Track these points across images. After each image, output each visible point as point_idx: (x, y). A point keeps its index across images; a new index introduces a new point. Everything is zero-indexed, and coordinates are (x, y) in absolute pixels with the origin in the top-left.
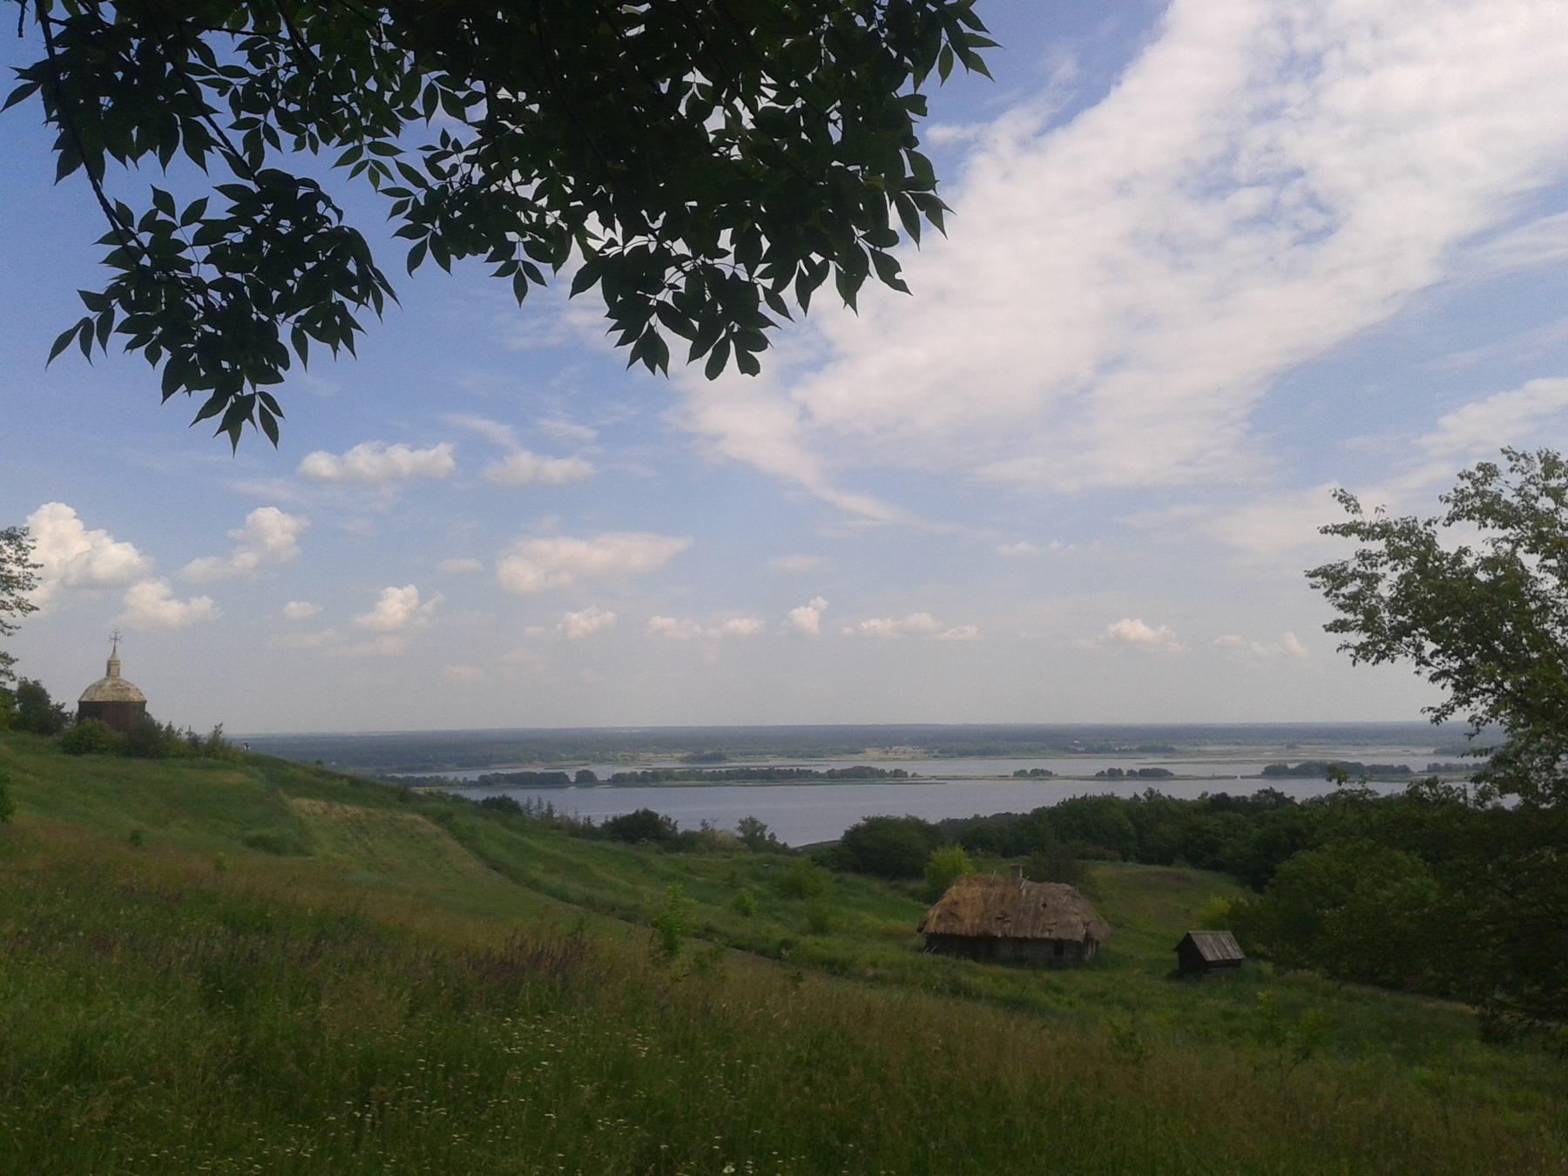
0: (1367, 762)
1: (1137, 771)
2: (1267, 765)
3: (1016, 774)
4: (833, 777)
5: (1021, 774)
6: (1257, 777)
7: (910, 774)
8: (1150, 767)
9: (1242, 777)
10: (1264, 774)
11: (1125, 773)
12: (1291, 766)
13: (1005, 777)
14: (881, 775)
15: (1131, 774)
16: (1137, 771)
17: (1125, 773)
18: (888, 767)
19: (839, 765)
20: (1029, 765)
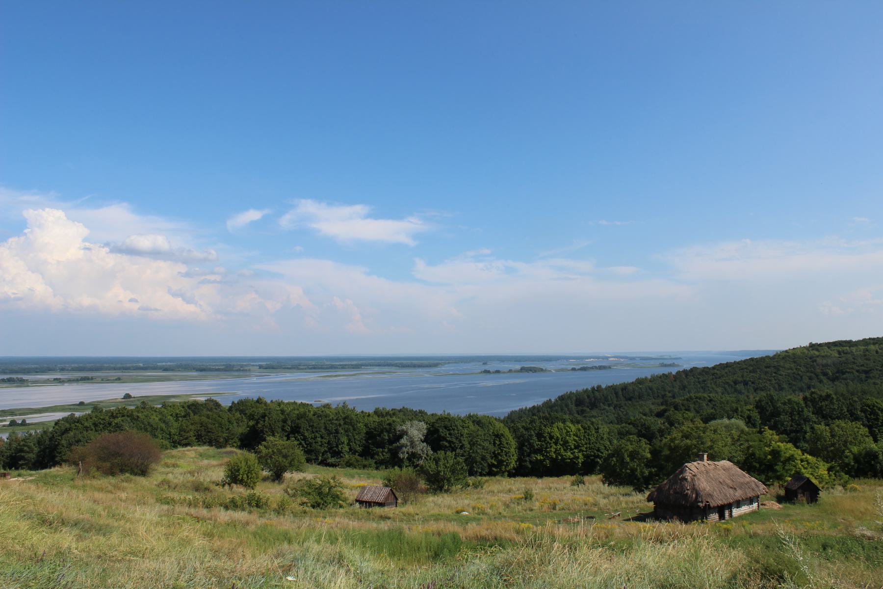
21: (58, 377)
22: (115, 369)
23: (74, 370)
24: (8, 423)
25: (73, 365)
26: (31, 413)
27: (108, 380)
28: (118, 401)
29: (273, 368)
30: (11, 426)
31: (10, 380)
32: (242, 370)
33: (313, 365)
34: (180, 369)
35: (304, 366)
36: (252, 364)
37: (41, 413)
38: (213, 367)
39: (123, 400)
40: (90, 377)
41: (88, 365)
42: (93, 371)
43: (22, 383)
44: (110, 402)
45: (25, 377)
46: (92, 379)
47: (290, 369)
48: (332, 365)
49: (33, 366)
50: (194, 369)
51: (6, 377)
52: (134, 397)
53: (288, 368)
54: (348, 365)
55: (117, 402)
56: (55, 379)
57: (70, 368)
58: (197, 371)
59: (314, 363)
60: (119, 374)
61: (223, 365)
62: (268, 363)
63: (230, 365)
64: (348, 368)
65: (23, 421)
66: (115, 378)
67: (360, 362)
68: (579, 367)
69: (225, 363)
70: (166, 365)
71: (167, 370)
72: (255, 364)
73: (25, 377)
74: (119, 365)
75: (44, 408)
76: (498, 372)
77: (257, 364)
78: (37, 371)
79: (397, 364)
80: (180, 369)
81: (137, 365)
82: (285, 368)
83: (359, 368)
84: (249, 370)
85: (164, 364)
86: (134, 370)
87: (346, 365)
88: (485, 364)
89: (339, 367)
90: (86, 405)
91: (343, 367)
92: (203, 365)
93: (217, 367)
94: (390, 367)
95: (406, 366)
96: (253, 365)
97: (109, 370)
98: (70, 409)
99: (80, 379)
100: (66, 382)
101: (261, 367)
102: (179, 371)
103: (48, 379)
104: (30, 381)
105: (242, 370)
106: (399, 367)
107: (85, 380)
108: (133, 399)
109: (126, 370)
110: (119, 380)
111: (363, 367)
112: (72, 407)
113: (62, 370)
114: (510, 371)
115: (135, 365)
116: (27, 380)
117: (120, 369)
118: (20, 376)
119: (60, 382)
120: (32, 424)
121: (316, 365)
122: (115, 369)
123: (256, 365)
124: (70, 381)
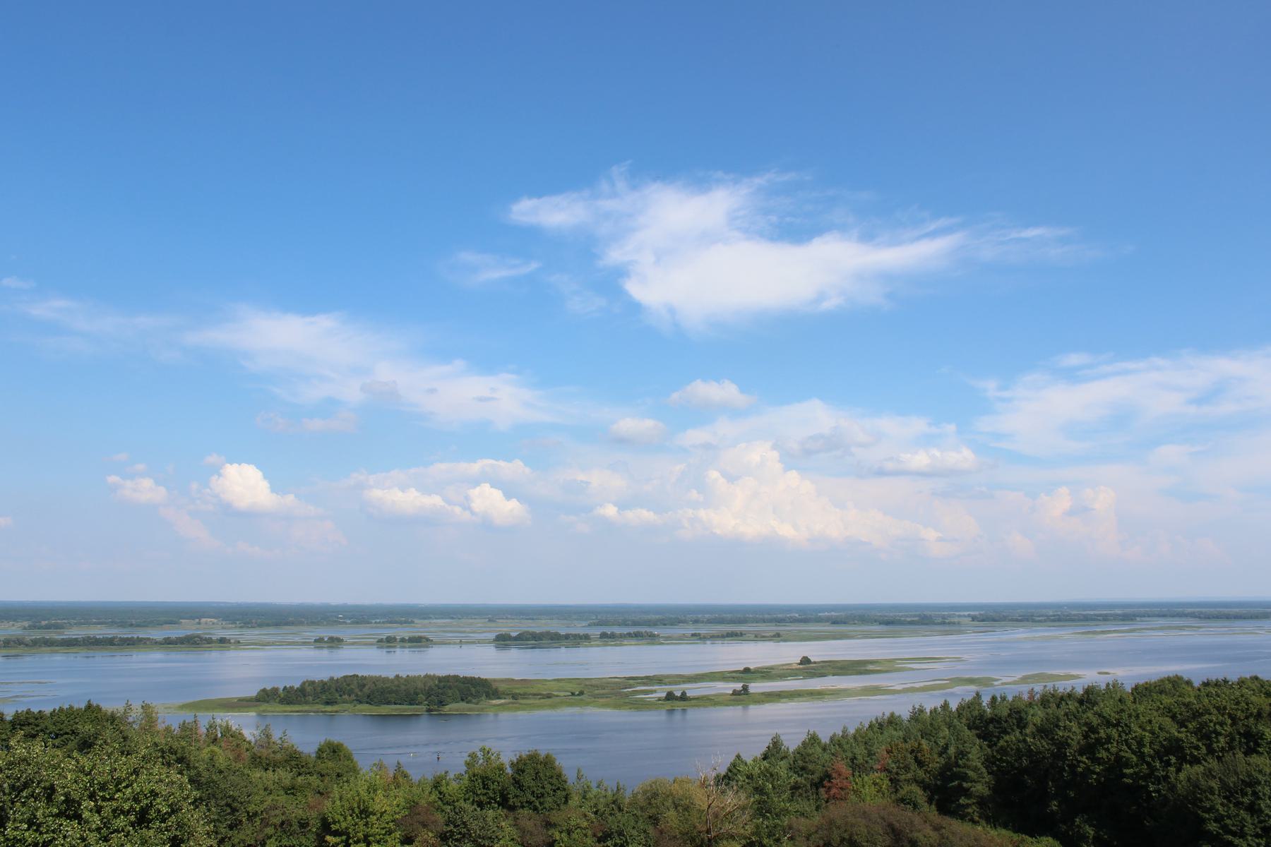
0: (538, 631)
1: (407, 638)
2: (497, 634)
3: (316, 641)
4: (168, 643)
7: (232, 641)
10: (495, 640)
11: (398, 640)
12: (514, 634)
14: (209, 641)
15: (403, 640)
16: (407, 638)
19: (175, 633)
20: (326, 632)
21: (697, 632)
22: (764, 622)
23: (710, 622)
24: (664, 695)
25: (707, 616)
26: (684, 682)
27: (764, 637)
28: (794, 668)
29: (994, 620)
30: (669, 700)
31: (637, 635)
32: (949, 623)
33: (1054, 616)
34: (856, 622)
35: (1039, 616)
36: (957, 613)
37: (696, 682)
38: (903, 619)
39: (801, 666)
40: (739, 632)
41: (729, 616)
42: (735, 623)
43: (652, 639)
44: (783, 669)
46: (741, 635)
47: (1021, 621)
48: (1084, 615)
49: (657, 617)
50: (875, 621)
51: (632, 630)
52: (815, 663)
53: (1017, 620)
54: (1111, 615)
55: (793, 669)
56: (693, 635)
57: (705, 620)
58: (880, 624)
59: (1051, 613)
60: (771, 629)
61: (915, 616)
62: (982, 612)
63: (925, 616)
64: (1115, 620)
65: (682, 694)
66: (772, 634)
67: (1128, 611)
69: (917, 613)
70: (832, 616)
71: (838, 623)
72: (962, 613)
74: (766, 616)
75: (697, 675)
77: (966, 613)
78: (663, 623)
79: (1194, 613)
80: (856, 622)
81: (792, 615)
82: (1012, 620)
83: (1132, 620)
84: (959, 623)
85: (826, 613)
86: (791, 622)
87: (1106, 615)
89: (1099, 618)
90: (753, 673)
91: (1105, 618)
92: (886, 616)
93: (909, 619)
94: (1184, 619)
95: (1214, 617)
96: (959, 616)
97: (757, 622)
98: (734, 678)
99: (725, 634)
100: (709, 639)
101: (974, 618)
102: (855, 624)
103: (684, 634)
104: (662, 637)
105: (949, 623)
106: (1200, 618)
107: (732, 636)
108: (814, 665)
109: (776, 621)
110: (777, 637)
111: (1138, 619)
112: (734, 674)
113: (696, 621)
115: (788, 615)
116: (658, 635)
117: (771, 621)
118: (649, 630)
119: (700, 639)
120: (694, 699)
121: (1058, 615)
122: (764, 621)
123: (965, 616)
124: (713, 637)
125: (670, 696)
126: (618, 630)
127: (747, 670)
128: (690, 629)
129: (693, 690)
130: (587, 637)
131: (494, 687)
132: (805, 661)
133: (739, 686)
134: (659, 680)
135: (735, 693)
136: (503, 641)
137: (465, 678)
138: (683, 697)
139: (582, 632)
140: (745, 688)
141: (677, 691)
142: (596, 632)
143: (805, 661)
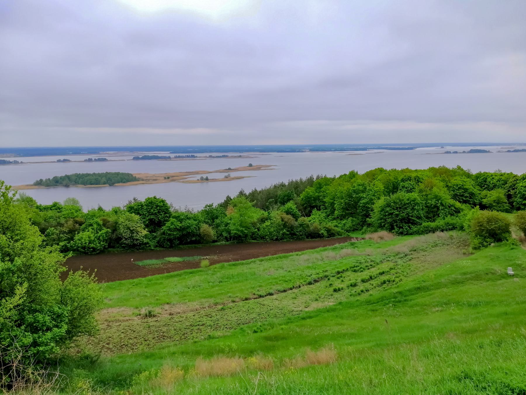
5: (59, 161)
6: (131, 160)
8: (101, 158)
9: (127, 160)
12: (140, 157)
13: (54, 162)
14: (9, 163)
17: (93, 160)
18: (12, 159)
20: (62, 158)
45: (195, 155)
46: (227, 156)
60: (239, 154)
68: (513, 150)
73: (195, 155)
76: (456, 152)
88: (442, 147)
113: (211, 151)
114: (464, 152)
116: (197, 156)
118: (193, 154)
120: (211, 179)
125: (202, 179)
126: (181, 155)
127: (230, 169)
128: (208, 155)
129: (210, 176)
130: (169, 158)
131: (134, 176)
132: (251, 165)
133: (226, 174)
134: (197, 173)
135: (226, 177)
136: (136, 158)
137: (122, 173)
138: (207, 179)
139: (167, 155)
140: (229, 176)
141: (205, 176)
142: (172, 155)
143: (251, 165)
